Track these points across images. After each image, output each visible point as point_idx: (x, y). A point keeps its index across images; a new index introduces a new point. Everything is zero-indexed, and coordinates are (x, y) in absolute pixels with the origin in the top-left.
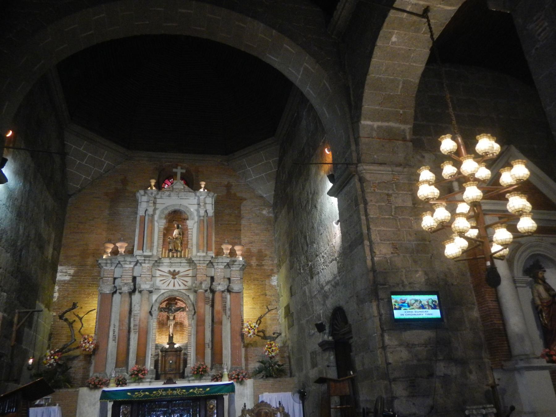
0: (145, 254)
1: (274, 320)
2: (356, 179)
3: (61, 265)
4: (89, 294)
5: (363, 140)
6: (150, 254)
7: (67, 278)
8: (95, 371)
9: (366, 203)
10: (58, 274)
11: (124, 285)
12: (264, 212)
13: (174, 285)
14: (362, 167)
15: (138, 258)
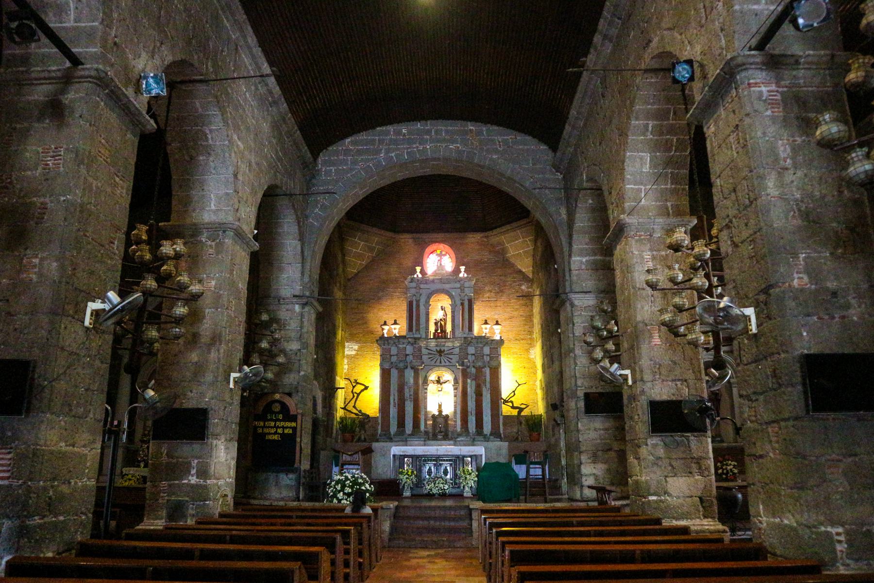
0: (416, 336)
1: (531, 390)
2: (568, 305)
3: (347, 342)
4: (371, 366)
5: (574, 273)
6: (419, 336)
7: (354, 353)
8: (382, 431)
9: (574, 325)
10: (346, 349)
11: (399, 363)
12: (523, 287)
13: (441, 362)
14: (572, 296)
15: (410, 340)
